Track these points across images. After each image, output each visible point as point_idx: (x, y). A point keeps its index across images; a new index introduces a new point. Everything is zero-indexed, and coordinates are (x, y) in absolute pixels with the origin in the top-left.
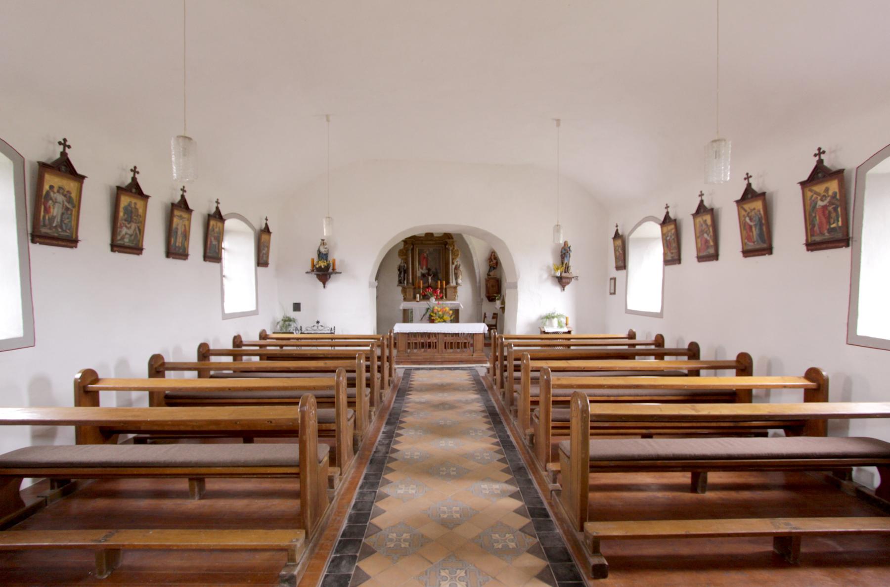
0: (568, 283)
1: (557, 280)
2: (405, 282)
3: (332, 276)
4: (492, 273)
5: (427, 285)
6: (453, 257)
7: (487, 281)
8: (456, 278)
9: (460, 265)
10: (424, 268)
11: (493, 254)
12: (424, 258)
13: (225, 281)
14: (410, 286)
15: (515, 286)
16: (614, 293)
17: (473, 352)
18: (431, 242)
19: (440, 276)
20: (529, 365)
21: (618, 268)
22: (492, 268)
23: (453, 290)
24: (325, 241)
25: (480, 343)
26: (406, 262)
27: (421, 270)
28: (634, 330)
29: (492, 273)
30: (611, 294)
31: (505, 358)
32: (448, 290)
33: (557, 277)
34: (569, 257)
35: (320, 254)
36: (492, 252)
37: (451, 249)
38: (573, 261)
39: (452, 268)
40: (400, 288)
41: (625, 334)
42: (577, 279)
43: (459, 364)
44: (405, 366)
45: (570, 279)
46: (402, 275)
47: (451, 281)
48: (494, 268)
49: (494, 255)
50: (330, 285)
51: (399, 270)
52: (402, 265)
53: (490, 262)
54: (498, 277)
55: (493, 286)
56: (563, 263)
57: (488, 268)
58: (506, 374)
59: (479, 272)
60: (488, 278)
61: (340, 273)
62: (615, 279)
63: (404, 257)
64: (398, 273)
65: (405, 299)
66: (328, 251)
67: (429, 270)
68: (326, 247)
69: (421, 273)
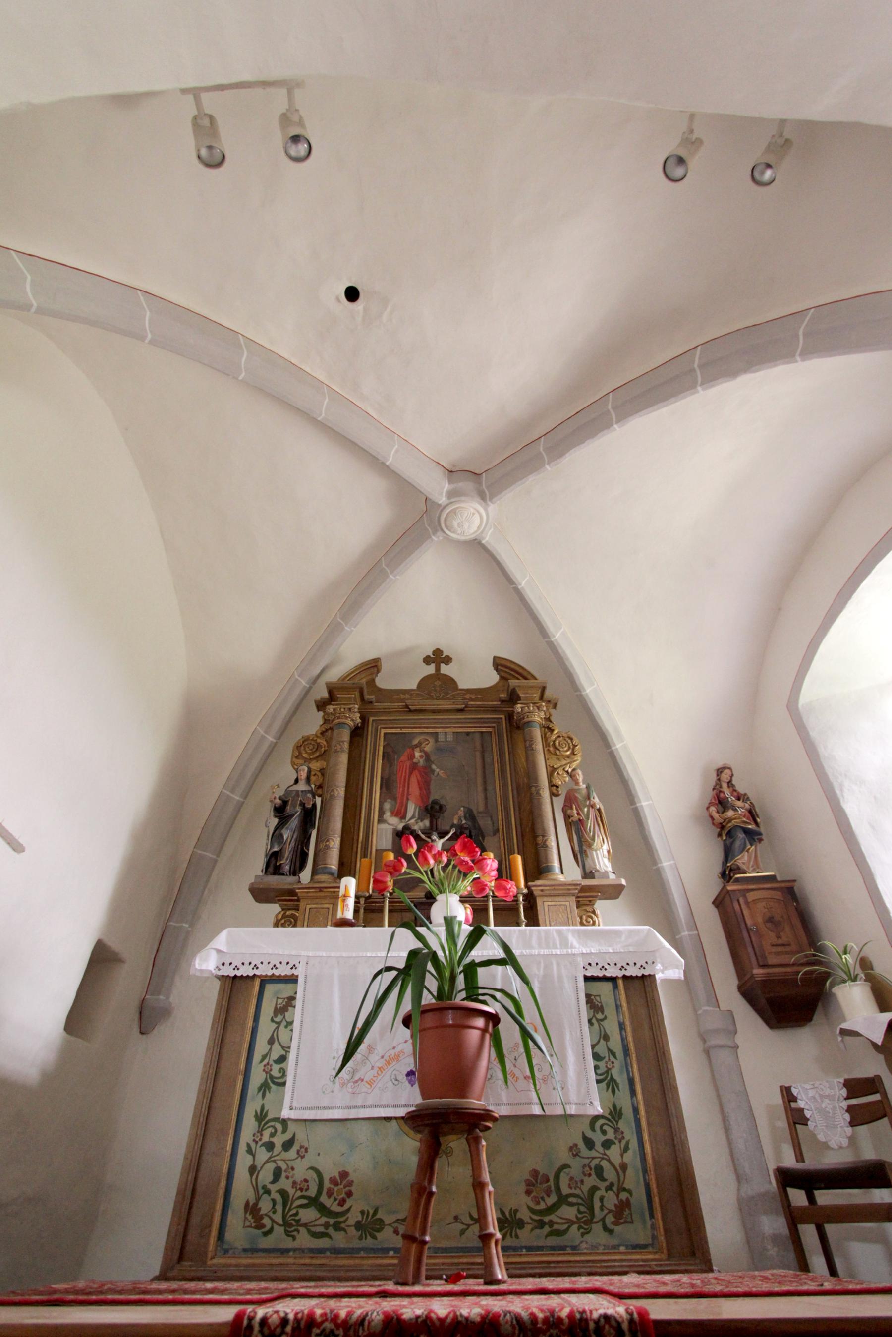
10: (412, 809)
12: (414, 767)
22: (741, 835)
36: (719, 771)
37: (538, 717)
47: (556, 864)
49: (730, 784)
51: (281, 811)
59: (676, 867)
63: (316, 766)
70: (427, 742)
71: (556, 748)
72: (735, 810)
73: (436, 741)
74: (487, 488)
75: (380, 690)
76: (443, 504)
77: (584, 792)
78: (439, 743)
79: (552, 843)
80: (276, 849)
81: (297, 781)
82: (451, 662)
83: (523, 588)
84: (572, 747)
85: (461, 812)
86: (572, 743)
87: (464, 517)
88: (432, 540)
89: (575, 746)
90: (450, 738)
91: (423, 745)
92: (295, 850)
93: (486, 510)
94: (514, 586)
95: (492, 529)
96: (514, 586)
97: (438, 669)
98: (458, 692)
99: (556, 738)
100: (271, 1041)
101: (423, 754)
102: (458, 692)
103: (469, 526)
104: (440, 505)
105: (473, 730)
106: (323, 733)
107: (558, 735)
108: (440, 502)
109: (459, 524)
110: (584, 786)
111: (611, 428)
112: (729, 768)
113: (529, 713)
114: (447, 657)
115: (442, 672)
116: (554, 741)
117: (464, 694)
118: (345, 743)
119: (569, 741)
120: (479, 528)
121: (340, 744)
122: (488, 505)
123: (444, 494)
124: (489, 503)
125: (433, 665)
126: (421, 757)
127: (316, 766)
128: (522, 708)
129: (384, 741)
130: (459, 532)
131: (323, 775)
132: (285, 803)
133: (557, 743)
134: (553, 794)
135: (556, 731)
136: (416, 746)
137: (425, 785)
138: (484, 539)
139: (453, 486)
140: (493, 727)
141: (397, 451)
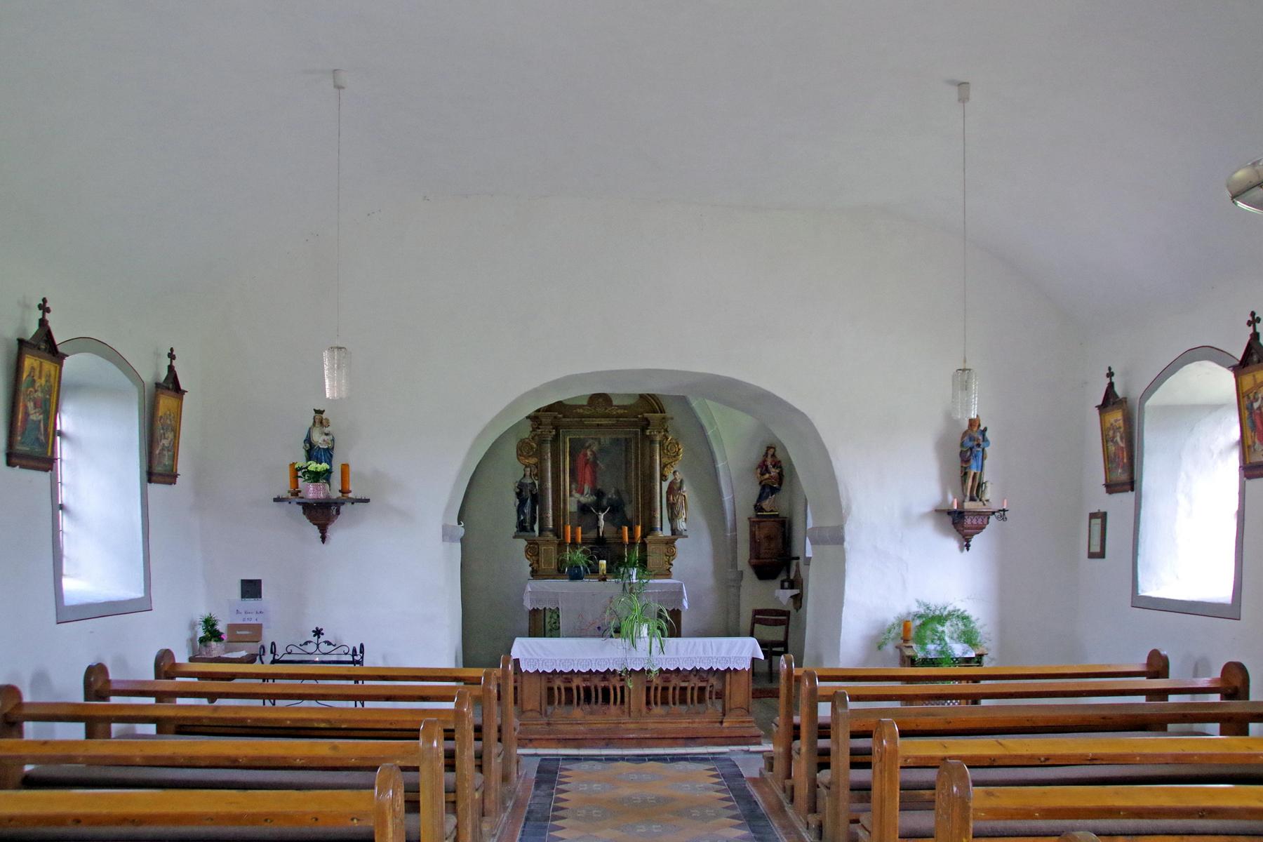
0: (980, 528)
1: (949, 519)
2: (536, 527)
3: (343, 508)
4: (766, 504)
5: (592, 534)
6: (665, 460)
7: (753, 523)
8: (673, 518)
9: (682, 481)
10: (587, 489)
11: (771, 452)
13: (65, 523)
14: (550, 536)
15: (836, 538)
16: (1102, 555)
17: (724, 715)
18: (604, 421)
19: (629, 511)
20: (896, 751)
21: (1111, 488)
22: (767, 490)
23: (664, 548)
24: (324, 416)
25: (739, 693)
26: (541, 475)
27: (577, 495)
28: (1163, 652)
29: (766, 504)
30: (1092, 556)
31: (824, 731)
32: (650, 548)
33: (950, 513)
34: (983, 458)
35: (312, 452)
36: (769, 448)
37: (658, 438)
38: (992, 470)
39: (661, 489)
40: (522, 544)
41: (1139, 663)
42: (1004, 518)
43: (686, 746)
44: (541, 751)
45: (987, 515)
46: (527, 510)
47: (659, 526)
48: (774, 491)
49: (773, 455)
50: (335, 532)
51: (519, 495)
52: (528, 481)
53: (762, 474)
54: (784, 512)
55: (769, 538)
56: (965, 475)
57: (756, 490)
58: (824, 776)
60: (757, 516)
61: (367, 501)
62: (1103, 516)
63: (533, 461)
64: (518, 503)
65: (535, 574)
66: (333, 440)
67: (599, 494)
68: (326, 430)
69: (579, 502)
72: (770, 473)
73: (599, 443)
77: (678, 485)
79: (658, 516)
80: (522, 518)
81: (525, 475)
85: (613, 491)
89: (679, 449)
90: (608, 442)
92: (531, 517)
100: (551, 618)
106: (533, 438)
110: (679, 481)
112: (774, 448)
116: (668, 446)
117: (617, 410)
126: (591, 455)
127: (533, 461)
128: (650, 432)
131: (537, 468)
132: (521, 490)
133: (669, 448)
134: (661, 480)
137: (594, 473)
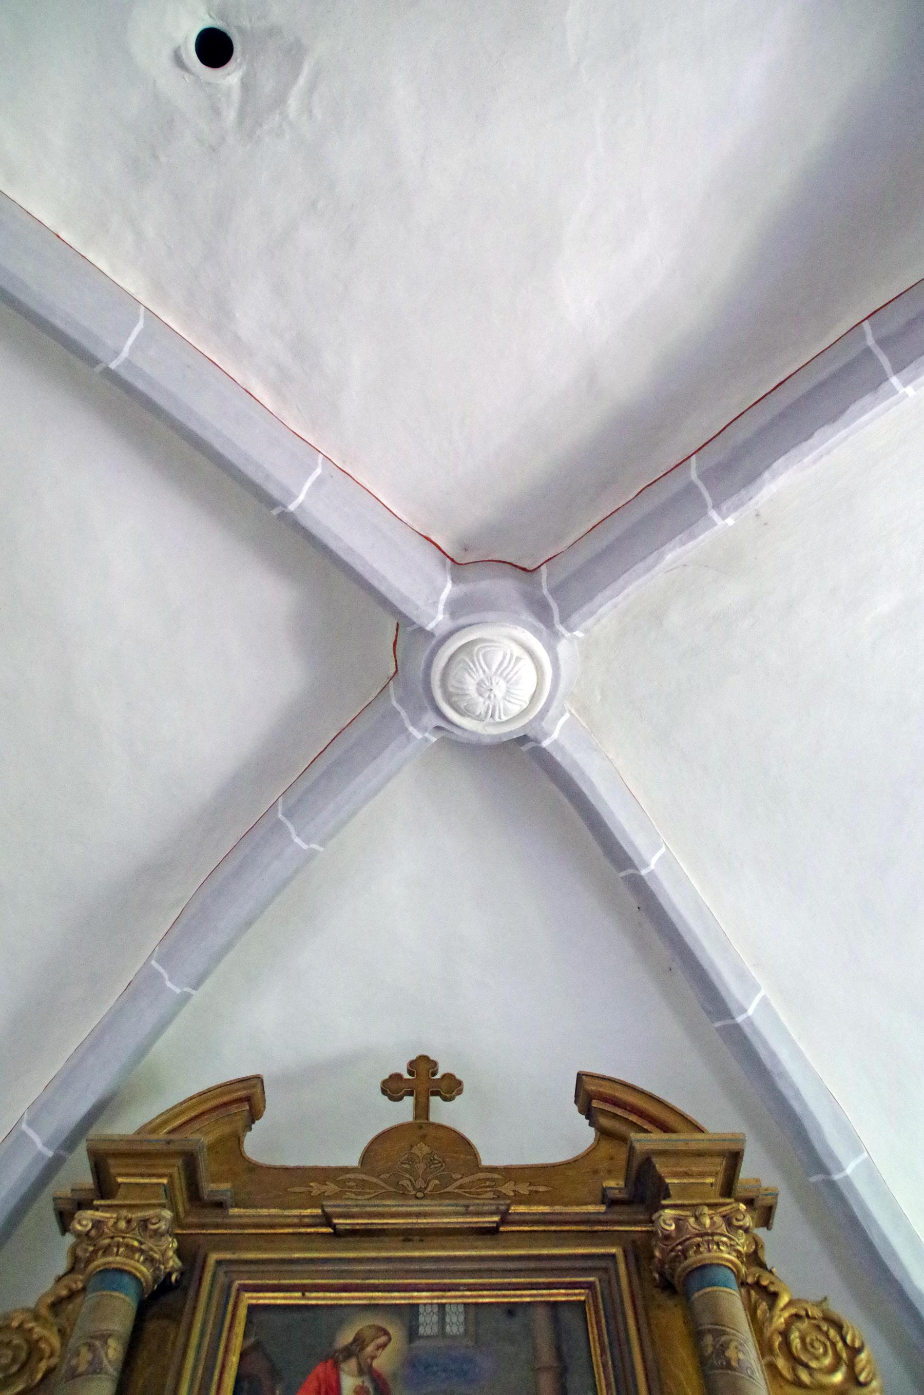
70: (383, 1339)
71: (795, 1361)
74: (553, 591)
75: (254, 1168)
76: (439, 633)
78: (417, 1343)
82: (460, 1092)
83: (651, 873)
84: (844, 1355)
86: (844, 1340)
87: (494, 668)
88: (409, 736)
89: (855, 1351)
90: (455, 1324)
91: (370, 1349)
93: (551, 650)
94: (631, 871)
95: (567, 716)
96: (631, 871)
97: (422, 1110)
98: (481, 1175)
99: (789, 1323)
101: (368, 1385)
102: (481, 1175)
103: (508, 692)
104: (431, 635)
105: (526, 1297)
107: (793, 1311)
108: (430, 627)
109: (480, 684)
111: (885, 387)
113: (701, 1235)
114: (449, 1077)
115: (433, 1118)
116: (785, 1334)
118: (112, 1342)
119: (832, 1333)
120: (534, 698)
121: (91, 1347)
122: (556, 635)
123: (441, 607)
124: (560, 628)
125: (409, 1101)
129: (246, 1335)
130: (480, 709)
133: (795, 1338)
135: (784, 1300)
136: (348, 1353)
138: (546, 735)
139: (463, 588)
140: (590, 1286)
141: (319, 482)
